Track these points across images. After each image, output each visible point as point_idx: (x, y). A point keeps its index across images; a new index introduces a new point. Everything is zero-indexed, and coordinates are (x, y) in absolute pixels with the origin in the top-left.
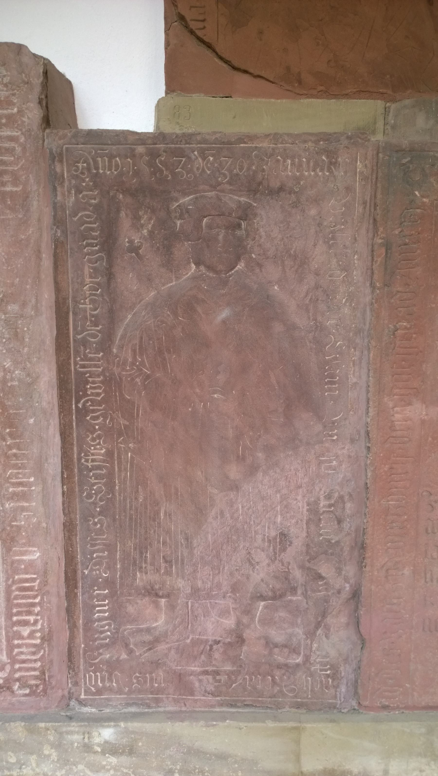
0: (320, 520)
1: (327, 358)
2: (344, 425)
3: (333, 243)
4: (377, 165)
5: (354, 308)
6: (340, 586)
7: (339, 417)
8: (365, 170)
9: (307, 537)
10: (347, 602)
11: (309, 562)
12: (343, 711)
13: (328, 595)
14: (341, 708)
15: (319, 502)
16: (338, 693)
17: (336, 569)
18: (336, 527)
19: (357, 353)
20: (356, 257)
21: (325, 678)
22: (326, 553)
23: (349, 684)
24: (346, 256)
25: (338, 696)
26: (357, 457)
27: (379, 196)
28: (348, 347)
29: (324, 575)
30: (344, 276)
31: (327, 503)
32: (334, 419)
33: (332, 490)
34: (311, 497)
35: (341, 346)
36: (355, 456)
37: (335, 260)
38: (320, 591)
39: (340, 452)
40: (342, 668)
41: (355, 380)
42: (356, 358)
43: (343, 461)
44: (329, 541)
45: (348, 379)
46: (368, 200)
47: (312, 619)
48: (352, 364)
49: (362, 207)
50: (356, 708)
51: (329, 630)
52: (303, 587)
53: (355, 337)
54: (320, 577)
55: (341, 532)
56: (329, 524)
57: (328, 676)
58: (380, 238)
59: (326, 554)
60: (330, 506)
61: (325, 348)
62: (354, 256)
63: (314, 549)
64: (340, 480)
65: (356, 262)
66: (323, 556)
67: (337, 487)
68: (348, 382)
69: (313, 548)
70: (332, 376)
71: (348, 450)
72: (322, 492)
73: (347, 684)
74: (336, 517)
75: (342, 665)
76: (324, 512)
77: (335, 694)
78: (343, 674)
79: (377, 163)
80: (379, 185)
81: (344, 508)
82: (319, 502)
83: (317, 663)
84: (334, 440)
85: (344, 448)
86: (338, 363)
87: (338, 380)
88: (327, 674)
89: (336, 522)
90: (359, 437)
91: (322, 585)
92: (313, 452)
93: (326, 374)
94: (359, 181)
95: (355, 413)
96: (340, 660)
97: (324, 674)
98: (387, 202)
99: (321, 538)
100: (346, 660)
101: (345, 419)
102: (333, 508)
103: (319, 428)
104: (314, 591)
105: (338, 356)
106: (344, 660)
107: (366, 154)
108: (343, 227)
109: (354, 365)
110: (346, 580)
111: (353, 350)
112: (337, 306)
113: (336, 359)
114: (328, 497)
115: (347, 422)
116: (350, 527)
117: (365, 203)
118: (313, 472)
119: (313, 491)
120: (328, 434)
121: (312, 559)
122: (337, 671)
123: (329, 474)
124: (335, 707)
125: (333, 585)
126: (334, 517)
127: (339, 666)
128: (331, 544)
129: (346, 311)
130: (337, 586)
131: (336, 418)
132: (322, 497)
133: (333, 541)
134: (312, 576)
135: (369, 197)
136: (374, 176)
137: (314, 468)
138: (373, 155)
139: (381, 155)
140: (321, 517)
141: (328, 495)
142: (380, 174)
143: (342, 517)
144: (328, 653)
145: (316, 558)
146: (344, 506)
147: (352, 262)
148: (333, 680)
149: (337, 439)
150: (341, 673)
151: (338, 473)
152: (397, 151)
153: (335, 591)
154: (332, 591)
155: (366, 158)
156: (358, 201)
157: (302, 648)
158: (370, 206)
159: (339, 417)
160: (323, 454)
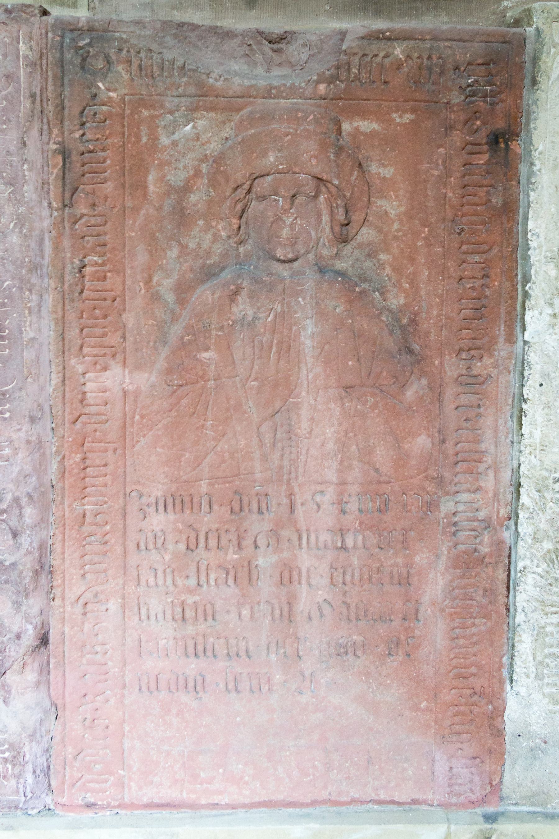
2: (19, 397)
4: (47, 47)
5: (26, 236)
6: (19, 628)
7: (11, 386)
8: (30, 53)
10: (33, 651)
12: (29, 812)
14: (26, 809)
16: (21, 786)
17: (13, 603)
18: (11, 542)
19: (34, 297)
20: (26, 167)
23: (38, 772)
24: (11, 166)
26: (40, 442)
27: (50, 88)
28: (20, 289)
30: (10, 193)
32: (5, 389)
33: (4, 489)
35: (9, 288)
36: (37, 442)
39: (14, 436)
40: (26, 749)
41: (32, 334)
42: (33, 304)
45: (21, 333)
46: (38, 92)
48: (27, 312)
49: (29, 101)
50: (52, 807)
51: (9, 692)
53: (29, 275)
55: (18, 550)
57: (6, 760)
58: (55, 143)
62: (23, 165)
64: (14, 475)
65: (26, 173)
67: (11, 486)
71: (27, 432)
73: (34, 772)
74: (10, 528)
75: (27, 743)
77: (17, 787)
78: (27, 757)
79: (47, 44)
80: (50, 73)
81: (21, 515)
84: (5, 419)
85: (20, 430)
87: (8, 333)
88: (4, 758)
89: (10, 536)
90: (42, 415)
94: (23, 68)
95: (34, 380)
96: (23, 736)
98: (61, 95)
100: (32, 736)
101: (21, 389)
102: (5, 515)
105: (6, 301)
106: (30, 736)
107: (31, 33)
108: (5, 127)
109: (30, 313)
110: (27, 618)
111: (27, 292)
115: (23, 393)
117: (33, 96)
122: (19, 753)
124: (16, 807)
125: (9, 627)
126: (7, 528)
127: (22, 745)
128: (4, 568)
129: (15, 239)
130: (15, 629)
131: (7, 388)
133: (7, 563)
135: (39, 88)
136: (44, 62)
138: (41, 34)
139: (50, 35)
142: (50, 59)
143: (19, 529)
146: (21, 512)
147: (20, 173)
148: (14, 765)
149: (10, 417)
150: (24, 756)
152: (72, 31)
153: (12, 636)
154: (8, 636)
155: (31, 39)
156: (24, 93)
158: (41, 101)
159: (11, 386)
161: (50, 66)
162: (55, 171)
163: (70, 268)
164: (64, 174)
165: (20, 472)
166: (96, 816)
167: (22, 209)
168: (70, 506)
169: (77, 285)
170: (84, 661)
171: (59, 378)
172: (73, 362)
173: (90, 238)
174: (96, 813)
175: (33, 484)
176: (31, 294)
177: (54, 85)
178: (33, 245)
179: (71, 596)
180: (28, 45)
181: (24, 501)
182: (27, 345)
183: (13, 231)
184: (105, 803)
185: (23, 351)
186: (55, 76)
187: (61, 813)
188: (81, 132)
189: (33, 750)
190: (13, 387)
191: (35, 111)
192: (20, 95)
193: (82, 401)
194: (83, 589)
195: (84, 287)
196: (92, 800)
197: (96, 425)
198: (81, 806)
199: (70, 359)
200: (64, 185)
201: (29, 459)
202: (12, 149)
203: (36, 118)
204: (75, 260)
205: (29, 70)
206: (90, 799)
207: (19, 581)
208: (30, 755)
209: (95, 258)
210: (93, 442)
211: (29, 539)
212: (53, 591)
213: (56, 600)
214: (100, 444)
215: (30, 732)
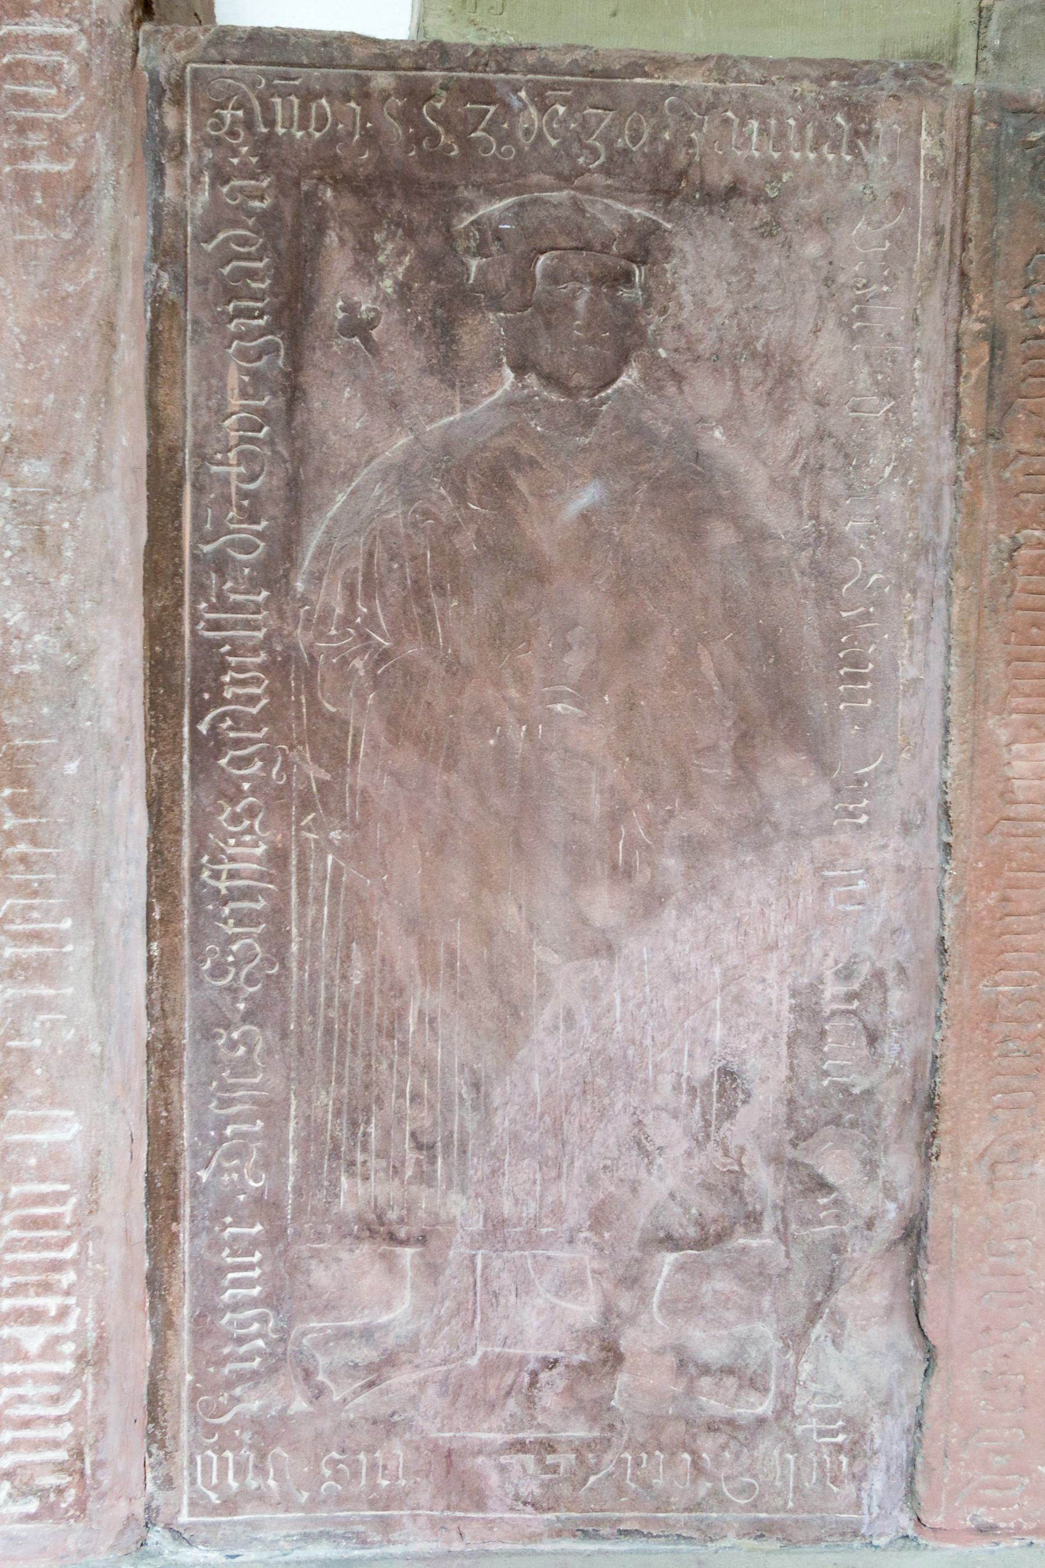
0: (823, 1033)
1: (844, 614)
3: (860, 329)
7: (872, 767)
9: (790, 1079)
11: (795, 1146)
13: (843, 1234)
15: (821, 987)
16: (864, 1495)
17: (864, 1163)
18: (865, 1052)
20: (917, 363)
21: (830, 1455)
22: (836, 1121)
23: (893, 1470)
24: (894, 361)
25: (865, 1502)
27: (974, 217)
28: (899, 587)
29: (831, 1179)
30: (888, 410)
31: (842, 989)
33: (855, 956)
34: (802, 975)
35: (879, 586)
37: (866, 370)
38: (821, 1223)
40: (874, 1428)
43: (883, 880)
44: (846, 1090)
45: (896, 669)
46: (948, 227)
47: (800, 1298)
49: (932, 243)
52: (779, 1213)
54: (823, 1186)
56: (846, 1045)
57: (839, 1448)
59: (838, 1125)
60: (850, 997)
61: (840, 589)
62: (912, 362)
63: (808, 1112)
64: (875, 929)
66: (831, 1129)
67: (869, 950)
68: (897, 677)
69: (804, 1108)
70: (857, 662)
72: (830, 961)
73: (888, 1468)
75: (876, 1418)
76: (833, 1013)
77: (858, 1496)
78: (878, 1441)
80: (973, 190)
81: (884, 1004)
82: (821, 987)
83: (811, 1415)
86: (873, 628)
87: (873, 670)
89: (864, 1041)
91: (825, 1207)
92: (806, 855)
93: (841, 655)
94: (925, 180)
97: (828, 1444)
99: (825, 1083)
102: (856, 1003)
103: (822, 793)
104: (805, 1223)
106: (881, 1404)
107: (942, 115)
108: (885, 288)
110: (889, 1192)
112: (871, 484)
113: (867, 617)
114: (846, 974)
116: (901, 1053)
117: (939, 232)
118: (806, 908)
119: (808, 958)
120: (845, 809)
121: (802, 1136)
122: (863, 1435)
123: (846, 914)
124: (855, 1534)
126: (860, 1026)
127: (868, 1421)
129: (893, 496)
130: (866, 1210)
131: (866, 770)
132: (829, 975)
134: (801, 1183)
135: (948, 219)
136: (962, 169)
137: (810, 899)
140: (827, 1027)
141: (845, 968)
143: (881, 1028)
144: (838, 1387)
145: (812, 1135)
146: (885, 998)
147: (908, 375)
148: (853, 1458)
149: (869, 824)
151: (870, 911)
156: (924, 227)
157: (773, 1376)
158: (952, 241)
159: (872, 767)
160: (831, 862)
161: (974, 177)
162: (975, 372)
163: (994, 551)
164: (991, 377)
165: (883, 925)
166: (996, 1548)
167: (907, 442)
168: (973, 987)
169: (1005, 582)
170: (986, 1269)
171: (964, 752)
172: (991, 723)
173: (1030, 495)
174: (997, 1544)
175: (906, 947)
176: (915, 598)
177: (981, 212)
178: (924, 508)
179: (970, 1151)
180: (937, 138)
181: (891, 977)
182: (905, 692)
183: (890, 480)
184: (1012, 1525)
185: (897, 702)
186: (983, 196)
187: (932, 1544)
188: (1024, 300)
189: (887, 1429)
190: (876, 769)
191: (940, 261)
192: (916, 233)
193: (1002, 795)
194: (991, 1137)
195: (1014, 585)
196: (990, 1520)
197: (1025, 839)
198: (969, 1530)
199: (985, 718)
200: (991, 396)
201: (901, 900)
202: (898, 330)
203: (940, 272)
204: (1002, 536)
205: (935, 184)
206: (985, 1519)
207: (876, 1122)
208: (882, 1438)
209: (1037, 533)
210: (1020, 870)
211: (896, 1047)
212: (936, 1142)
213: (941, 1157)
214: (1031, 874)
215: (881, 1396)
